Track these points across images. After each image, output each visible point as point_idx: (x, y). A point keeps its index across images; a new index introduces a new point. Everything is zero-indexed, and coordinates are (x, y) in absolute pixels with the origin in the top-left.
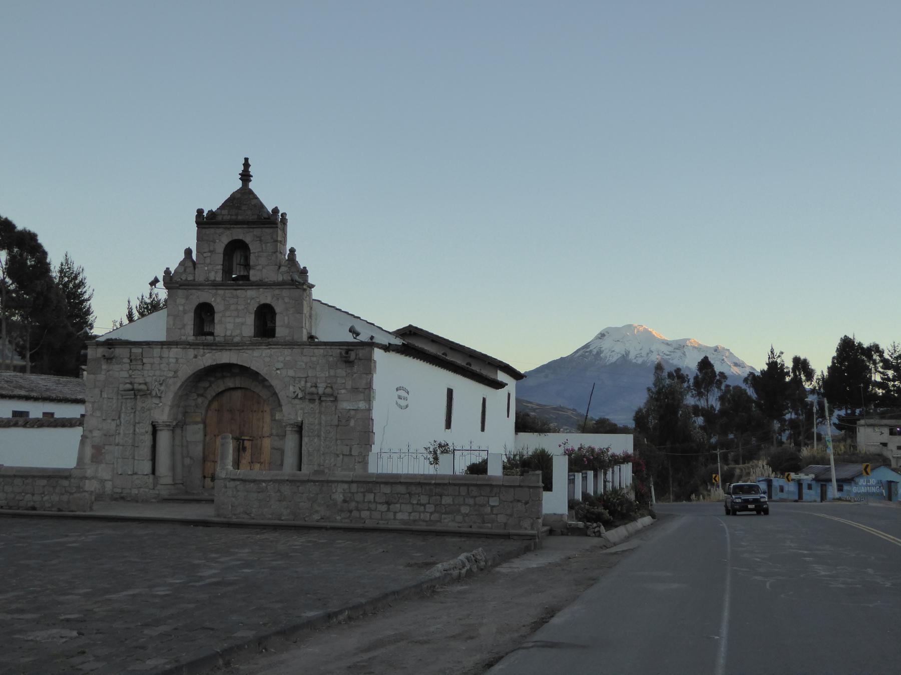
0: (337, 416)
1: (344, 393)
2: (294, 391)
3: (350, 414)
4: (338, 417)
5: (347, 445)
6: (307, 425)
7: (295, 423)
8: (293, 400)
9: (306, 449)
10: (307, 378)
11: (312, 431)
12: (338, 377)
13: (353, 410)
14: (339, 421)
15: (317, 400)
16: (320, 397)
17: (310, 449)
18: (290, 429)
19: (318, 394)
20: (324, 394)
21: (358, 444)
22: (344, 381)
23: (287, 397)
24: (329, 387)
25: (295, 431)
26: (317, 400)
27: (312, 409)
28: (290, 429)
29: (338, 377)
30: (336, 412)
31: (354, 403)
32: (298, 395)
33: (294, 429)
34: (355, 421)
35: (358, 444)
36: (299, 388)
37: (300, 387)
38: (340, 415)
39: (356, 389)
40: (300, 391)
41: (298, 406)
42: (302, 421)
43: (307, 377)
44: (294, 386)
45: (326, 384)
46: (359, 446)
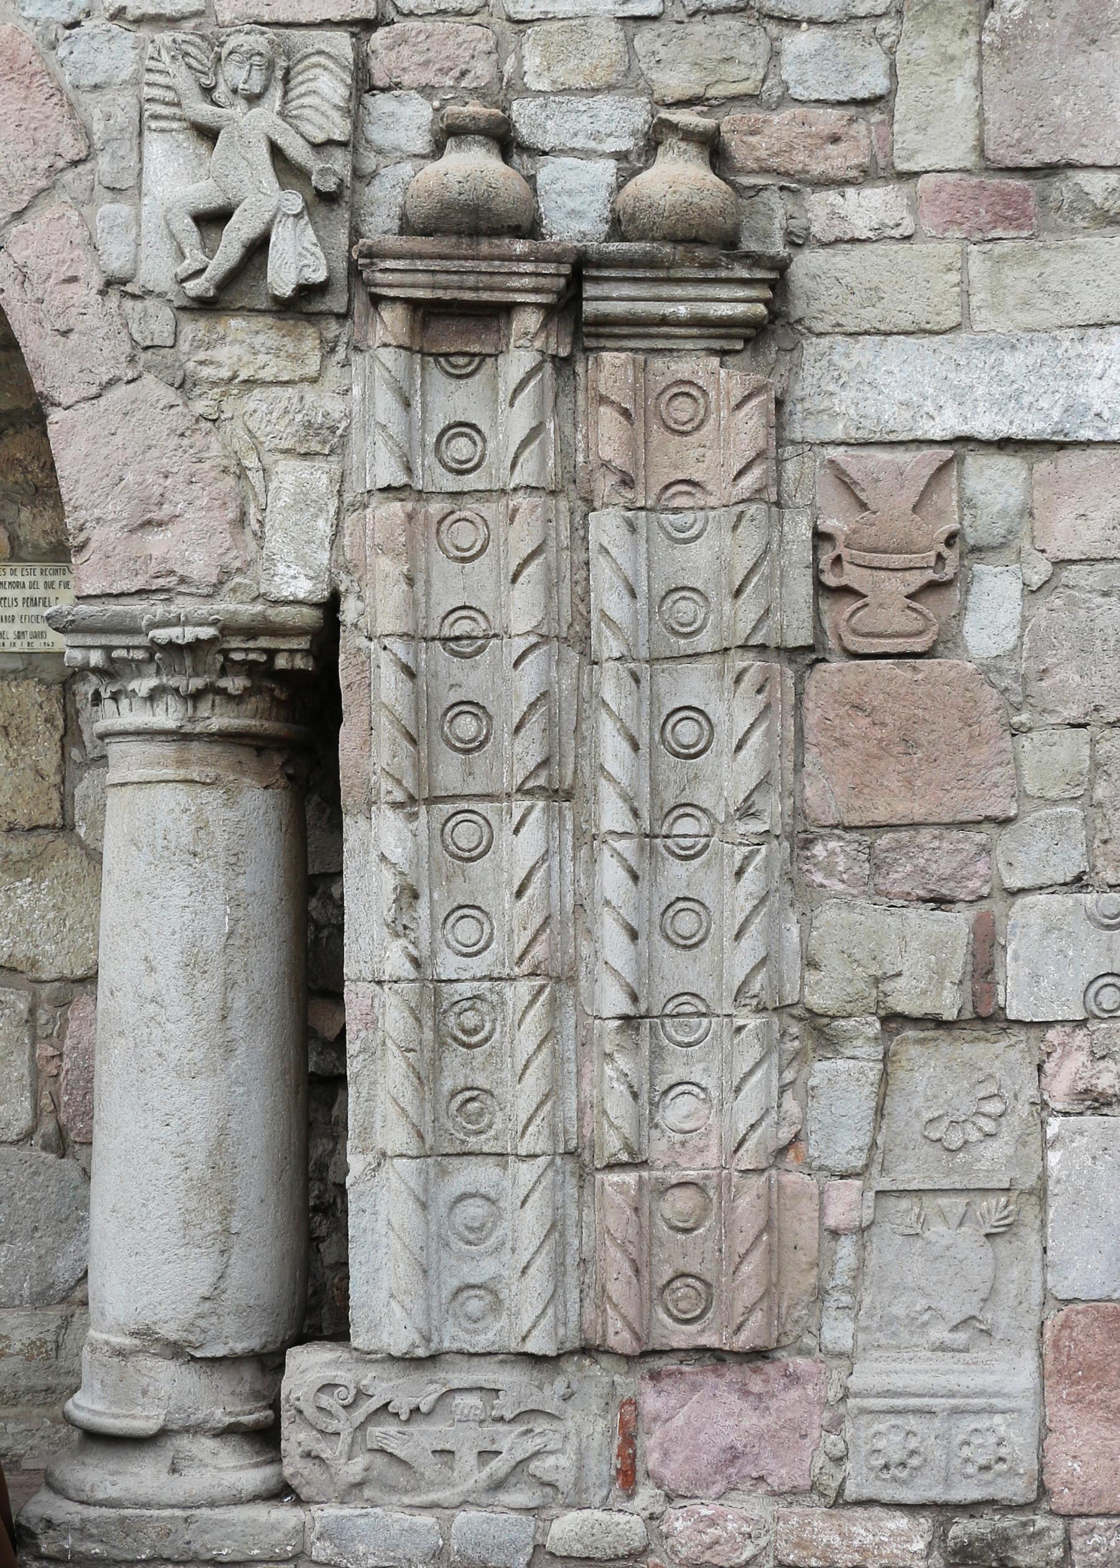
0: (800, 530)
1: (879, 237)
2: (206, 196)
3: (966, 503)
4: (820, 537)
5: (941, 902)
6: (398, 647)
7: (227, 629)
8: (193, 329)
9: (396, 962)
10: (379, 37)
11: (467, 726)
12: (791, 22)
13: (1005, 444)
14: (820, 587)
15: (528, 321)
16: (576, 278)
17: (448, 965)
18: (167, 715)
19: (532, 229)
20: (618, 227)
21: (1078, 883)
22: (873, 82)
23: (112, 283)
24: (689, 135)
25: (225, 737)
26: (528, 321)
27: (461, 448)
28: (167, 715)
29: (791, 22)
30: (780, 462)
31: (1013, 363)
32: (258, 248)
33: (219, 719)
34: (1031, 592)
35: (1078, 883)
36: (276, 152)
37: (297, 151)
38: (830, 524)
39: (1050, 170)
40: (295, 201)
41: (256, 400)
42: (331, 605)
43: (368, 25)
44: (208, 134)
45: (639, 116)
46: (1088, 899)
